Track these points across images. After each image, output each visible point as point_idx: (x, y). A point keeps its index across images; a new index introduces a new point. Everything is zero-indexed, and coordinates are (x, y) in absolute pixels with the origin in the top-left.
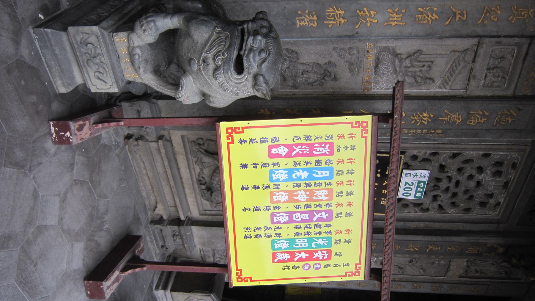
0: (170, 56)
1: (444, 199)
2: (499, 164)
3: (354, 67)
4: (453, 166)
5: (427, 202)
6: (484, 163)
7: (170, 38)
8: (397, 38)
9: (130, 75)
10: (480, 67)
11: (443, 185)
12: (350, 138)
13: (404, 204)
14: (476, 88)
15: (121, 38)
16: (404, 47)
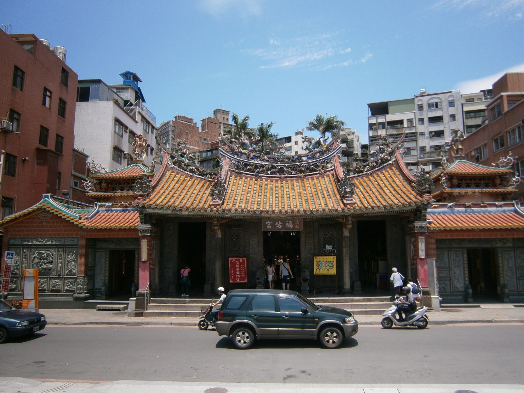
7: (303, 279)
9: (307, 285)
12: (317, 259)
15: (303, 285)
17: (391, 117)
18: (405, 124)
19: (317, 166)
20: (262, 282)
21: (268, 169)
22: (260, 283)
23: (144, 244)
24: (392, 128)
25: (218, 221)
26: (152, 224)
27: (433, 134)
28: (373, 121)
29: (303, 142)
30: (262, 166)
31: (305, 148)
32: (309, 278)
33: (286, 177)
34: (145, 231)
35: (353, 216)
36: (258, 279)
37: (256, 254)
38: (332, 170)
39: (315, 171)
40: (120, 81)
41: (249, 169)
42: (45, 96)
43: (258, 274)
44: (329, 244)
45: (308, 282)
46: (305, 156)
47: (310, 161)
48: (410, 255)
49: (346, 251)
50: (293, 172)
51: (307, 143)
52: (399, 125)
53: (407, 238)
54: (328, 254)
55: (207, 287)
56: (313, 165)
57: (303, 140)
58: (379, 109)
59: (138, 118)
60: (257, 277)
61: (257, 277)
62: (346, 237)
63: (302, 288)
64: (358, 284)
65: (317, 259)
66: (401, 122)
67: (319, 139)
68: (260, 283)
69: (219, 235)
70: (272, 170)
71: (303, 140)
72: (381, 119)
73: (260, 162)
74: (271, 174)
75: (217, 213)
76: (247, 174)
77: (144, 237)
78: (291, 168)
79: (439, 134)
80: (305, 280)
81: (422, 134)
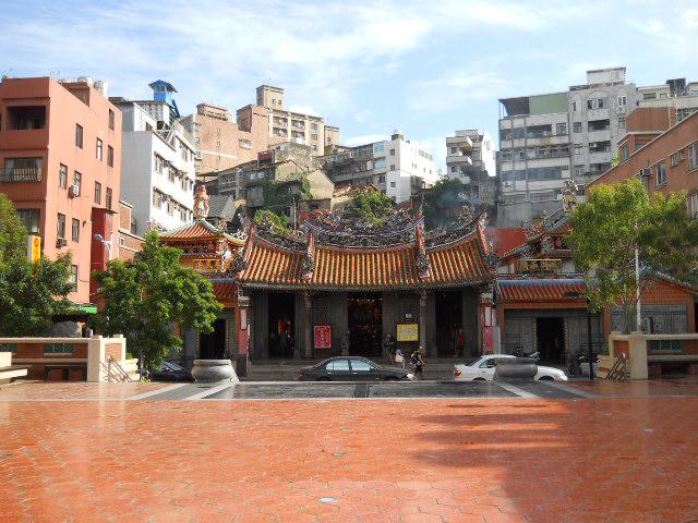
12: (399, 326)
17: (535, 120)
18: (554, 131)
19: (399, 237)
23: (243, 314)
24: (536, 137)
26: (250, 296)
27: (595, 146)
28: (507, 125)
30: (346, 237)
34: (244, 302)
40: (149, 95)
42: (97, 146)
48: (480, 323)
52: (545, 133)
53: (479, 308)
54: (411, 321)
55: (296, 353)
58: (517, 106)
59: (177, 143)
64: (434, 351)
65: (399, 326)
66: (548, 127)
69: (308, 305)
72: (519, 123)
77: (243, 308)
79: (602, 146)
81: (579, 146)
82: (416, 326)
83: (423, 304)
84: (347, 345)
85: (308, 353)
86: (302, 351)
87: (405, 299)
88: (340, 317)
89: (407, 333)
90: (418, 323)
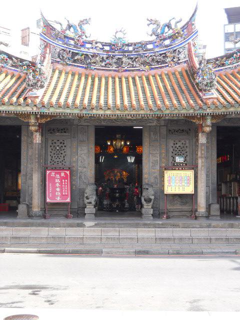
0: (148, 200)
1: (183, 152)
2: (174, 144)
3: (154, 173)
4: (175, 152)
5: (184, 156)
6: (174, 146)
7: (145, 200)
8: (149, 166)
9: (150, 207)
10: (155, 152)
11: (179, 153)
13: (185, 160)
14: (158, 152)
15: (145, 207)
16: (151, 164)
20: (93, 203)
21: (103, 60)
22: (90, 203)
25: (37, 119)
29: (148, 25)
31: (150, 33)
32: (152, 197)
33: (126, 71)
35: (213, 117)
36: (88, 199)
37: (85, 167)
38: (185, 62)
39: (164, 62)
41: (78, 59)
43: (87, 191)
44: (179, 155)
45: (151, 203)
46: (150, 42)
47: (157, 50)
49: (202, 162)
50: (135, 63)
51: (153, 27)
55: (22, 208)
56: (161, 55)
57: (149, 22)
60: (86, 195)
61: (86, 195)
62: (203, 145)
63: (143, 210)
64: (216, 207)
67: (170, 21)
68: (90, 203)
69: (37, 138)
70: (107, 61)
71: (149, 22)
73: (91, 51)
74: (105, 66)
75: (35, 109)
76: (75, 66)
78: (132, 58)
80: (148, 200)
82: (190, 173)
83: (202, 139)
84: (93, 199)
85: (36, 208)
86: (29, 207)
87: (181, 128)
88: (84, 158)
89: (178, 182)
90: (194, 167)
